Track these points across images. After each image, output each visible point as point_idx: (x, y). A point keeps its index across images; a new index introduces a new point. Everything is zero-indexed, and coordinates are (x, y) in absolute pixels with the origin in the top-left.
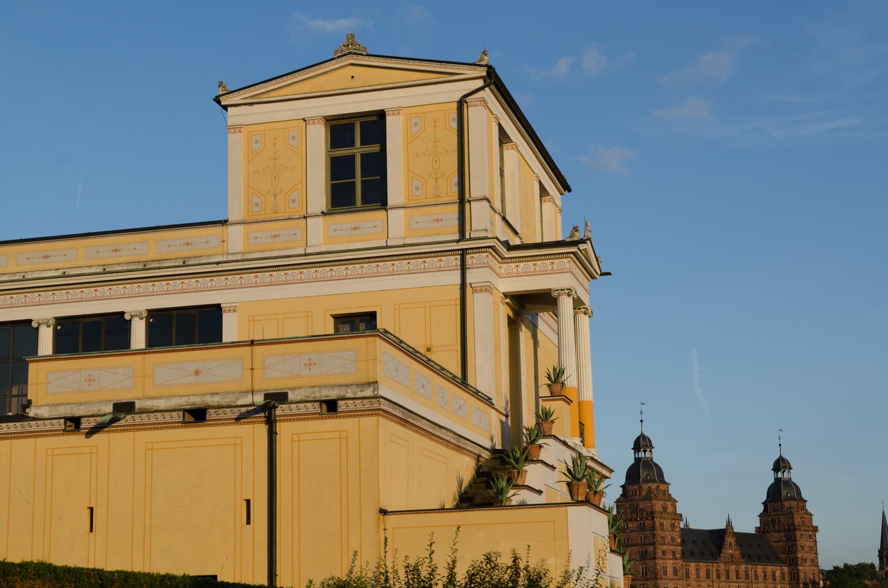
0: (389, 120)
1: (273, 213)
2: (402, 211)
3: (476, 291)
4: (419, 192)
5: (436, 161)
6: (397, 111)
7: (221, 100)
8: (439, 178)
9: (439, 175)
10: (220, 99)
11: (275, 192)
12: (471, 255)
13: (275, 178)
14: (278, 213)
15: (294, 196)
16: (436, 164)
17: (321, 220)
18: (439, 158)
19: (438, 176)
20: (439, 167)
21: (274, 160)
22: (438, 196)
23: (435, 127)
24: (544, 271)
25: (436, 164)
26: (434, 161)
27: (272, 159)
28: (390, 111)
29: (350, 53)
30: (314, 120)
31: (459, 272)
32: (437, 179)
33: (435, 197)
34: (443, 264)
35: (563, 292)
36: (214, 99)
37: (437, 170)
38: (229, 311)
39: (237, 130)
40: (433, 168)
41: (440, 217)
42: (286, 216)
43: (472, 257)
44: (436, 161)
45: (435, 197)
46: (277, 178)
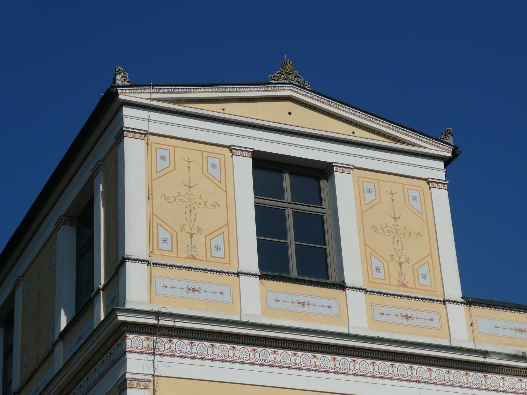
0: (339, 177)
1: (188, 258)
2: (362, 294)
6: (349, 168)
7: (119, 91)
9: (403, 259)
10: (117, 90)
13: (190, 211)
14: (196, 259)
15: (218, 241)
17: (257, 279)
21: (188, 189)
26: (396, 242)
27: (185, 185)
28: (339, 166)
29: (290, 83)
30: (242, 150)
32: (401, 264)
38: (138, 387)
46: (193, 212)
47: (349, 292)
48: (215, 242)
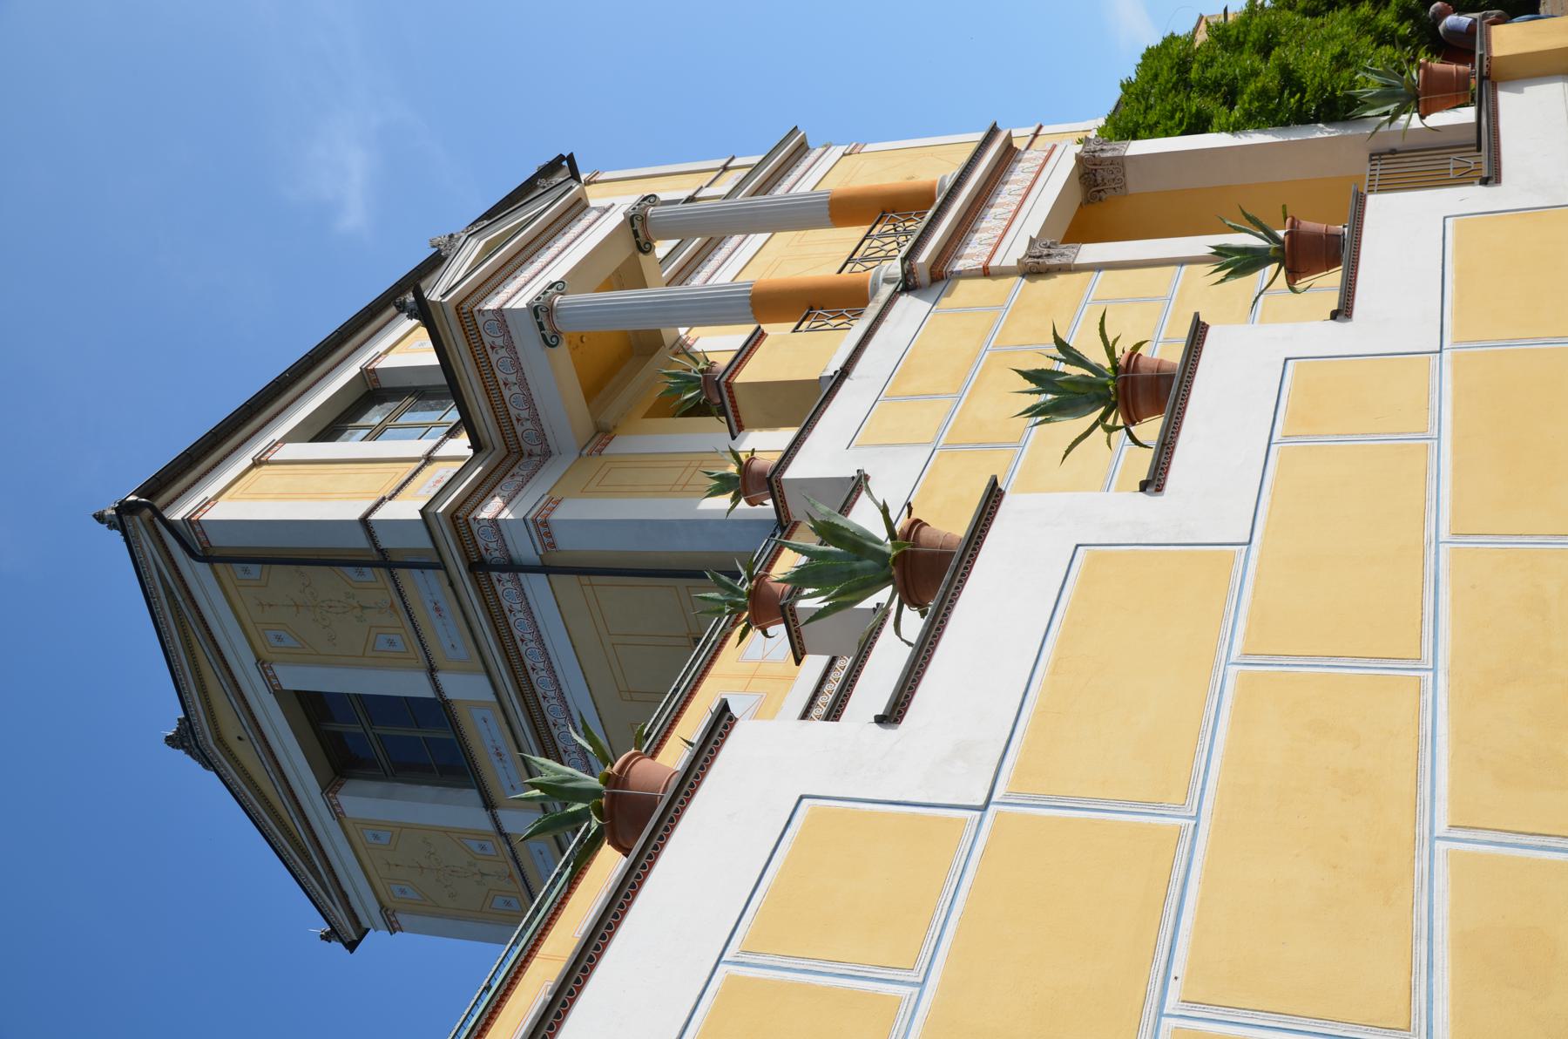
3: (553, 545)
4: (397, 639)
5: (330, 607)
8: (358, 602)
11: (476, 874)
12: (483, 552)
16: (335, 607)
18: (323, 602)
19: (356, 605)
20: (339, 601)
22: (392, 605)
23: (271, 605)
24: (513, 365)
25: (335, 607)
26: (331, 610)
31: (522, 576)
33: (396, 611)
34: (518, 607)
35: (546, 325)
36: (352, 952)
37: (345, 605)
39: (393, 919)
40: (344, 613)
41: (430, 606)
42: (511, 863)
43: (487, 550)
44: (330, 607)
45: (396, 611)
47: (450, 694)
48: (478, 850)
